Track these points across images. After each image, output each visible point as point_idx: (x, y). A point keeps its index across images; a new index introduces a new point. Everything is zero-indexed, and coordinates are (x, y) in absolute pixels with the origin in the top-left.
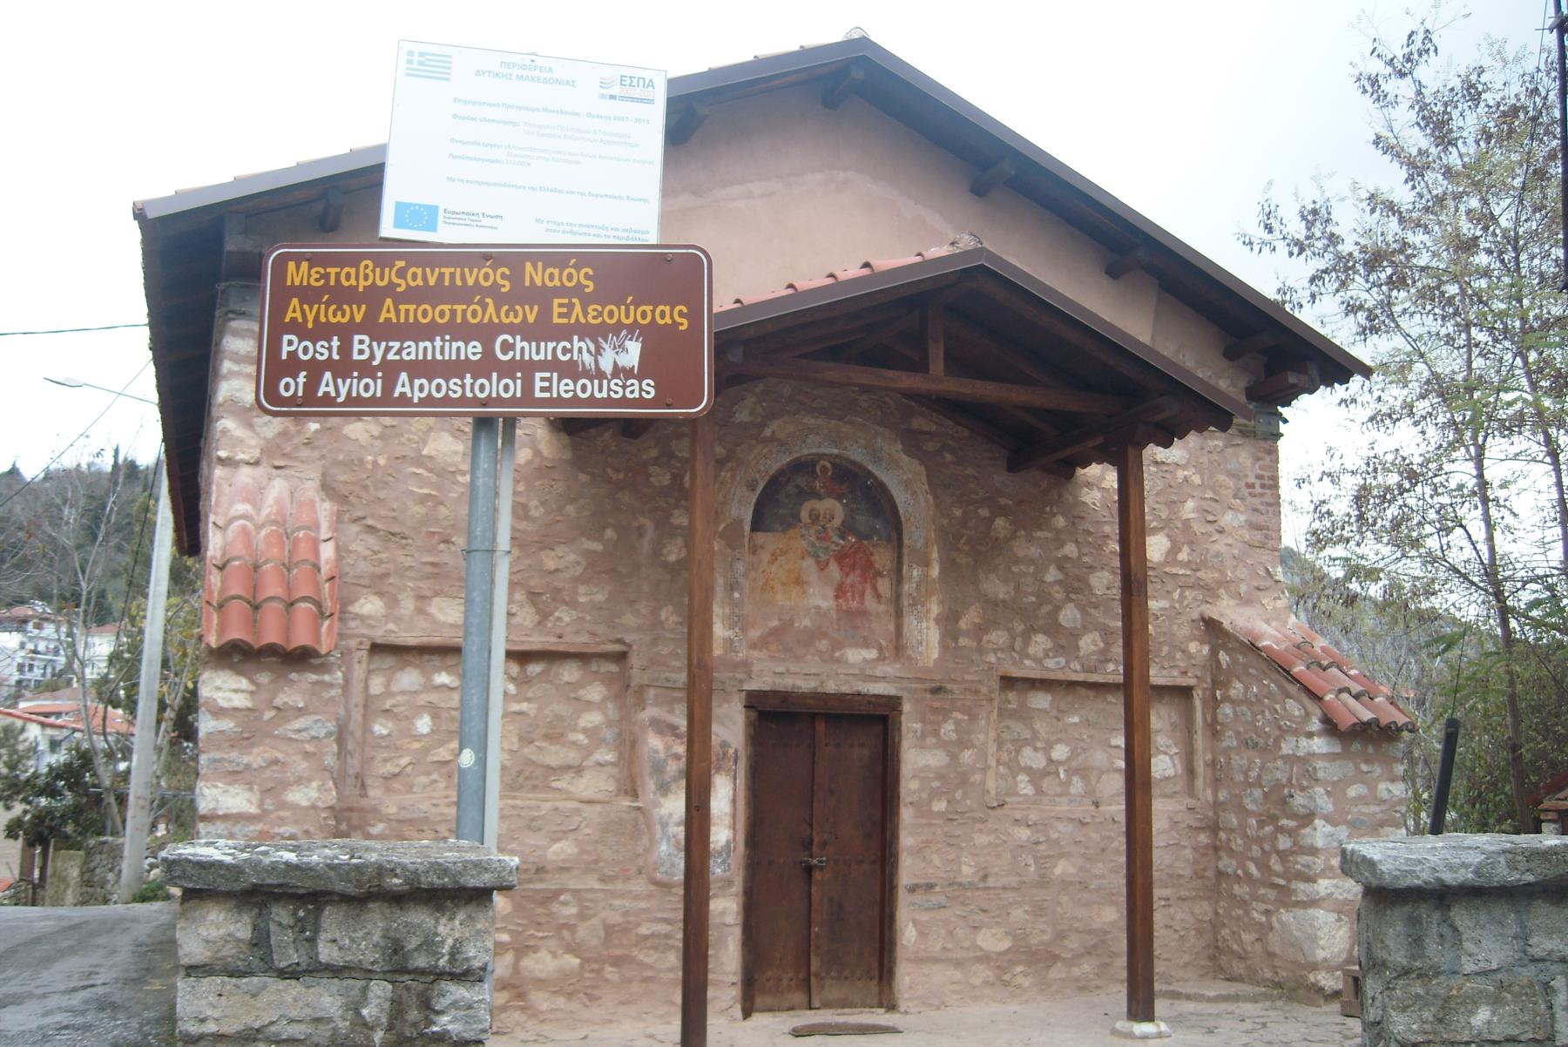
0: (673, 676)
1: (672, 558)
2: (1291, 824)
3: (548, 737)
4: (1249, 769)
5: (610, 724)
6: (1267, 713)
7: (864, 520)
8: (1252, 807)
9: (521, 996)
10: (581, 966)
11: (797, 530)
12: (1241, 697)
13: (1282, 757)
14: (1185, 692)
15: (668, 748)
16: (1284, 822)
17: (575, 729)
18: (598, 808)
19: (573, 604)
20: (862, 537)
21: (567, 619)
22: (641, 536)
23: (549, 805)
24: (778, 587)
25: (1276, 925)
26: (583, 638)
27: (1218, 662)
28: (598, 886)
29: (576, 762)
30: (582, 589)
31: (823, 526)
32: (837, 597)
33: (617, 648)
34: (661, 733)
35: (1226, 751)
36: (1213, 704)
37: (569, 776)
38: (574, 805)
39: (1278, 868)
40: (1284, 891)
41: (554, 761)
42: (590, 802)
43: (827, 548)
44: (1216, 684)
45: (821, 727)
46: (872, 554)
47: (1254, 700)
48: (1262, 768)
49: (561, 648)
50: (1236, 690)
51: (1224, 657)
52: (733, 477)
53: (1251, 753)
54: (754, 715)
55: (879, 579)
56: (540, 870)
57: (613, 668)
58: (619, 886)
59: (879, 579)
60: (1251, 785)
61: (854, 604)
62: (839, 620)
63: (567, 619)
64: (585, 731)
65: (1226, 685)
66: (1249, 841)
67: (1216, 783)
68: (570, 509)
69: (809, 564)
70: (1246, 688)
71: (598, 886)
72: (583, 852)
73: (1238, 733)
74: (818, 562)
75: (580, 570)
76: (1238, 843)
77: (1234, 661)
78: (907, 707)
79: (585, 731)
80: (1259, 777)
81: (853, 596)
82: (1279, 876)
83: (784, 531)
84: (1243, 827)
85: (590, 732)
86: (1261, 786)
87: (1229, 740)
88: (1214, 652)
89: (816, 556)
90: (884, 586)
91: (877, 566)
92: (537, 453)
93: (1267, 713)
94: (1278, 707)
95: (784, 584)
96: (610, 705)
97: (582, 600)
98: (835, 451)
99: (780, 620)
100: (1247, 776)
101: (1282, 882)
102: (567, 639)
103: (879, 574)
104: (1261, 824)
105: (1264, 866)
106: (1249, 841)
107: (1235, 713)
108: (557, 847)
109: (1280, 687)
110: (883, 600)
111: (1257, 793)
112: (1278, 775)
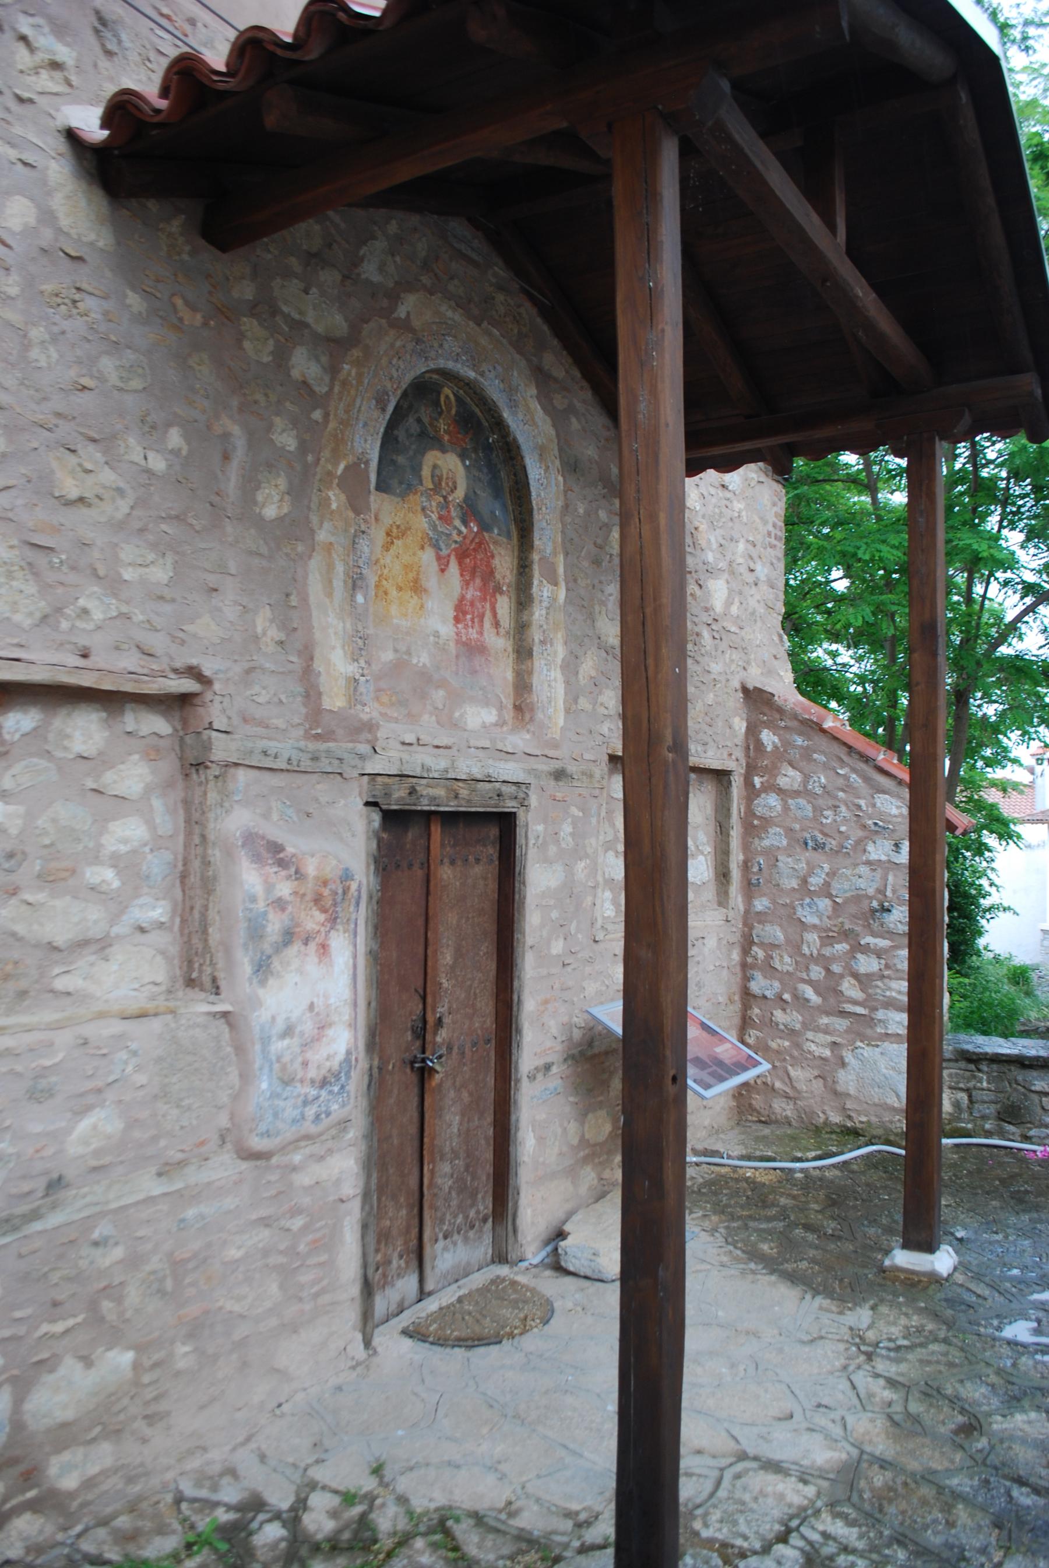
0: (273, 746)
1: (271, 512)
2: (883, 943)
3: (47, 879)
4: (811, 872)
5: (157, 842)
6: (843, 809)
7: (486, 503)
8: (811, 919)
9: (30, 1476)
10: (136, 1366)
11: (417, 497)
12: (796, 787)
13: (869, 863)
14: (721, 776)
15: (269, 887)
16: (869, 940)
17: (95, 858)
18: (155, 1025)
19: (114, 585)
20: (484, 527)
21: (98, 615)
22: (226, 457)
23: (64, 1038)
24: (393, 593)
25: (849, 1057)
26: (130, 661)
27: (759, 745)
28: (158, 1188)
29: (96, 932)
30: (128, 552)
31: (445, 498)
32: (457, 620)
33: (187, 685)
34: (257, 859)
35: (772, 855)
36: (751, 793)
37: (84, 961)
38: (117, 1027)
39: (856, 994)
40: (869, 1021)
41: (60, 932)
42: (142, 1015)
43: (449, 535)
44: (751, 770)
45: (436, 830)
46: (493, 557)
47: (819, 791)
48: (832, 874)
49: (86, 681)
50: (789, 777)
51: (768, 738)
52: (360, 376)
53: (817, 857)
54: (376, 818)
55: (498, 596)
56: (56, 1184)
57: (156, 724)
58: (194, 1176)
59: (498, 596)
60: (811, 894)
61: (473, 634)
62: (457, 657)
63: (98, 615)
64: (116, 861)
65: (772, 771)
66: (805, 962)
67: (750, 888)
68: (108, 365)
69: (428, 556)
70: (807, 778)
71: (158, 1188)
72: (132, 1124)
73: (789, 831)
74: (439, 558)
75: (123, 507)
76: (785, 962)
77: (787, 744)
78: (533, 800)
79: (116, 861)
80: (827, 884)
81: (472, 620)
82: (856, 1003)
83: (403, 496)
84: (795, 947)
85: (121, 863)
86: (830, 896)
87: (774, 838)
88: (752, 731)
89: (437, 547)
90: (504, 605)
91: (498, 576)
92: (47, 216)
93: (843, 809)
94: (862, 803)
95: (400, 589)
96: (157, 804)
97: (128, 574)
98: (472, 374)
99: (396, 651)
100: (804, 881)
101: (860, 1010)
102: (97, 660)
103: (498, 589)
104: (828, 940)
105: (829, 988)
106: (805, 962)
107: (786, 808)
108: (85, 1125)
109: (867, 779)
110: (502, 631)
111: (824, 904)
112: (861, 883)
